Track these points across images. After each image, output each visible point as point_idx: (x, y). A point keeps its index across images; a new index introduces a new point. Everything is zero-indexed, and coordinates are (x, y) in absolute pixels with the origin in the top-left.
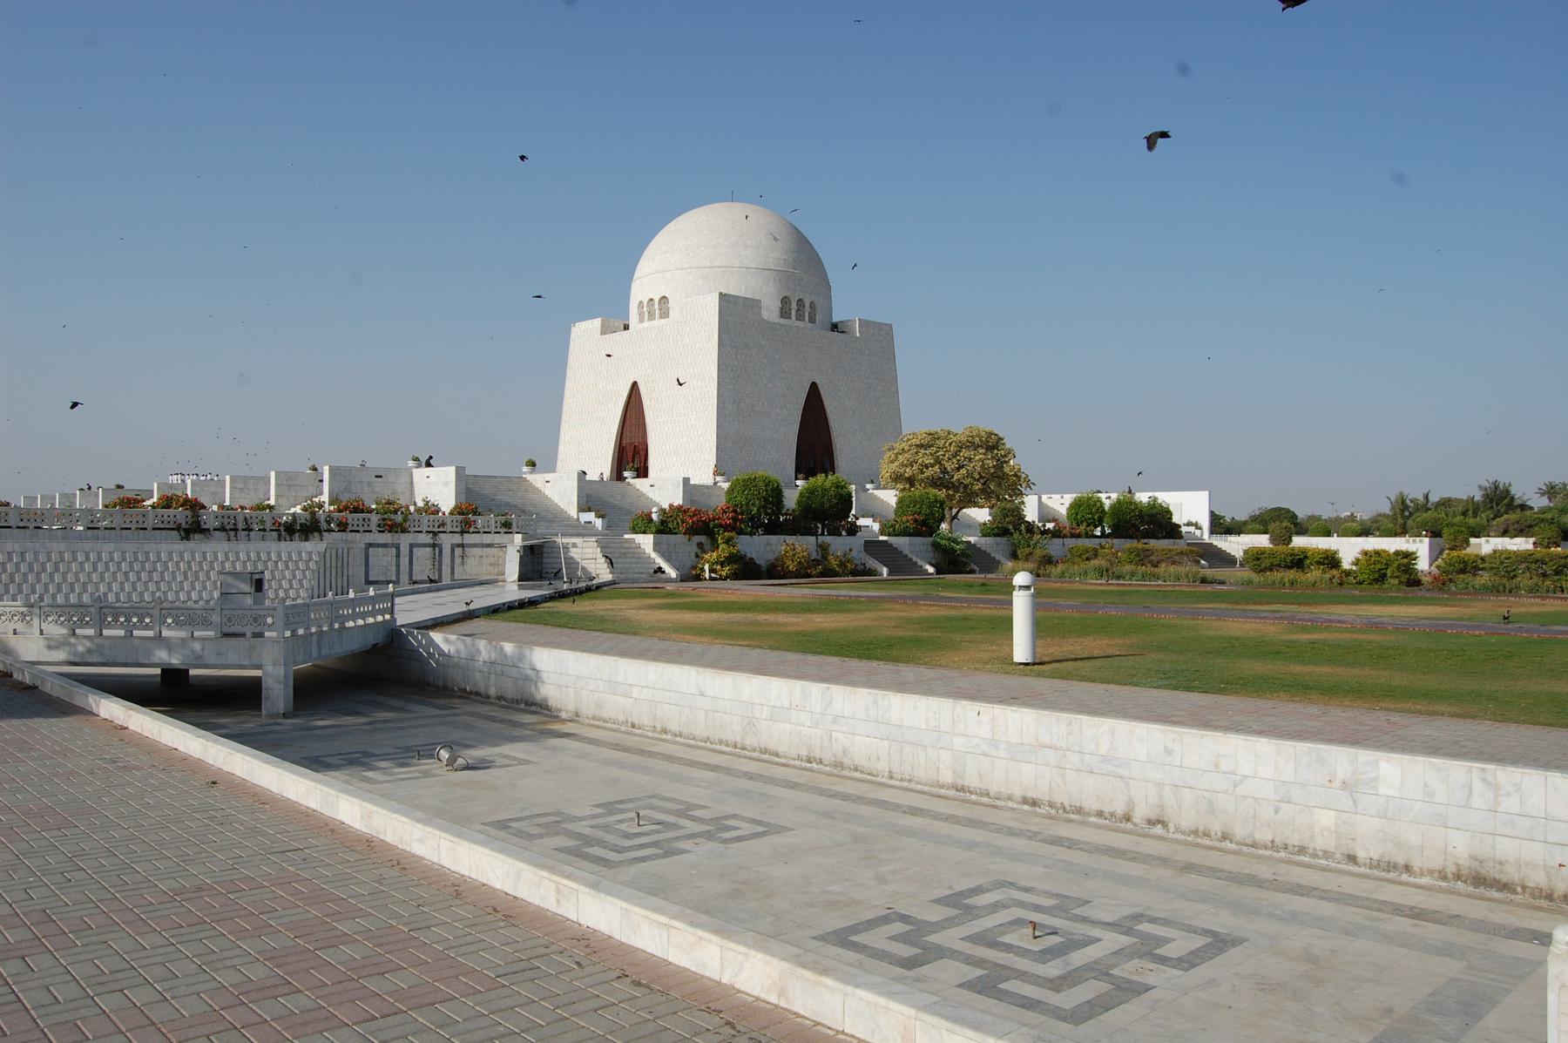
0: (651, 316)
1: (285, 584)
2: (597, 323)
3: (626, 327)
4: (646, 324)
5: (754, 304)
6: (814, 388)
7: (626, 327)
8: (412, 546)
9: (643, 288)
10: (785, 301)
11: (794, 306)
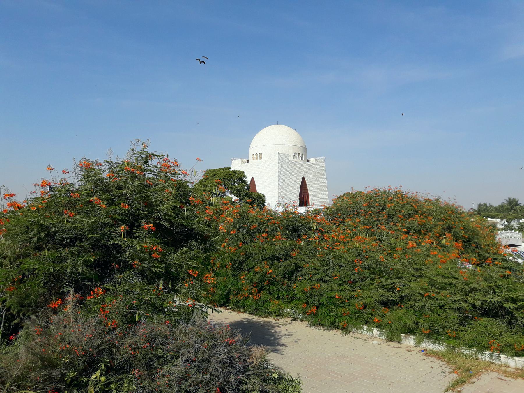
0: (257, 159)
2: (240, 160)
4: (255, 161)
5: (287, 156)
6: (303, 178)
7: (248, 161)
9: (253, 150)
11: (297, 155)
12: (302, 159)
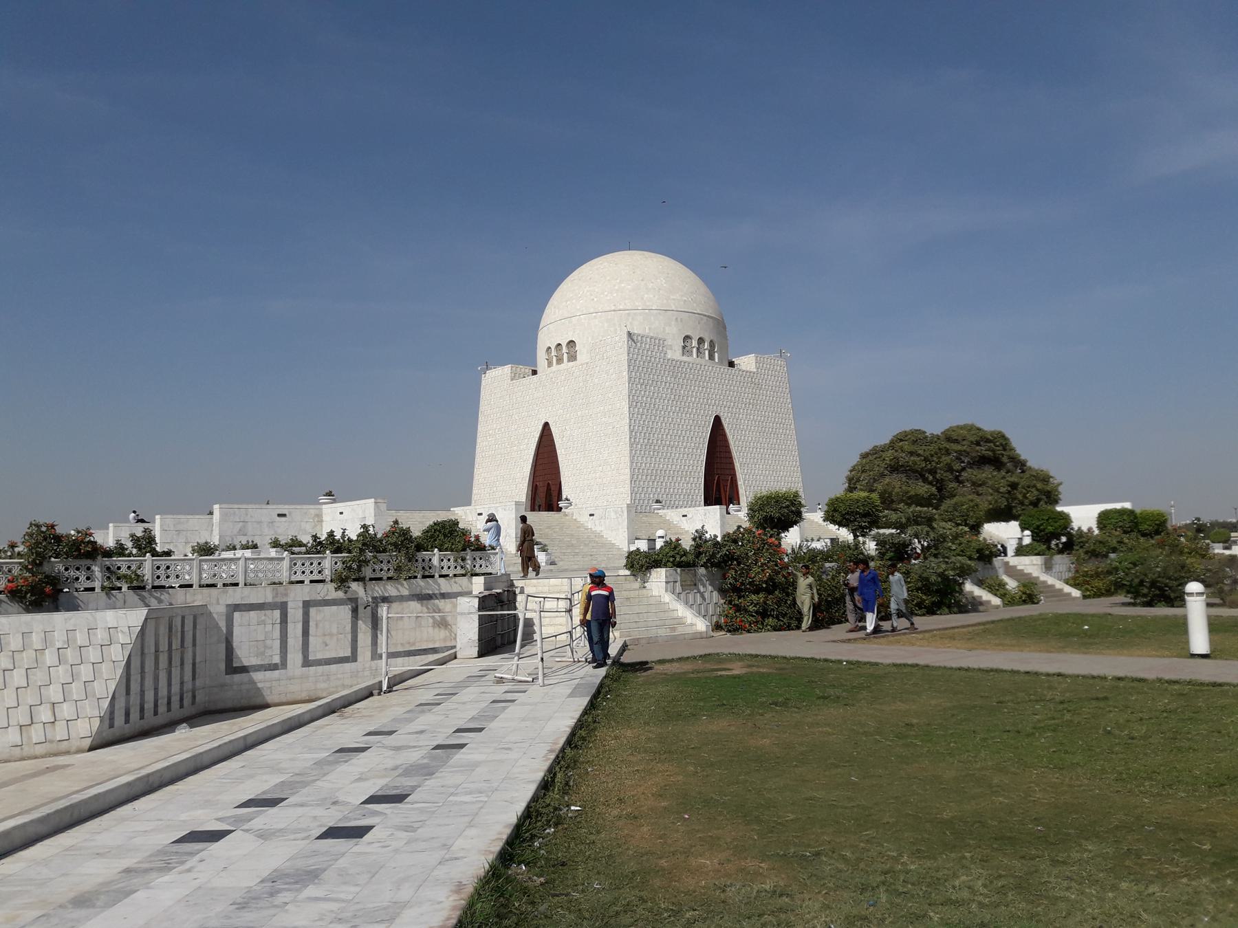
0: (560, 361)
1: (54, 693)
2: (507, 369)
3: (534, 373)
4: (555, 367)
5: (659, 343)
7: (534, 373)
8: (307, 605)
9: (551, 332)
10: (687, 338)
11: (695, 343)
12: (711, 357)
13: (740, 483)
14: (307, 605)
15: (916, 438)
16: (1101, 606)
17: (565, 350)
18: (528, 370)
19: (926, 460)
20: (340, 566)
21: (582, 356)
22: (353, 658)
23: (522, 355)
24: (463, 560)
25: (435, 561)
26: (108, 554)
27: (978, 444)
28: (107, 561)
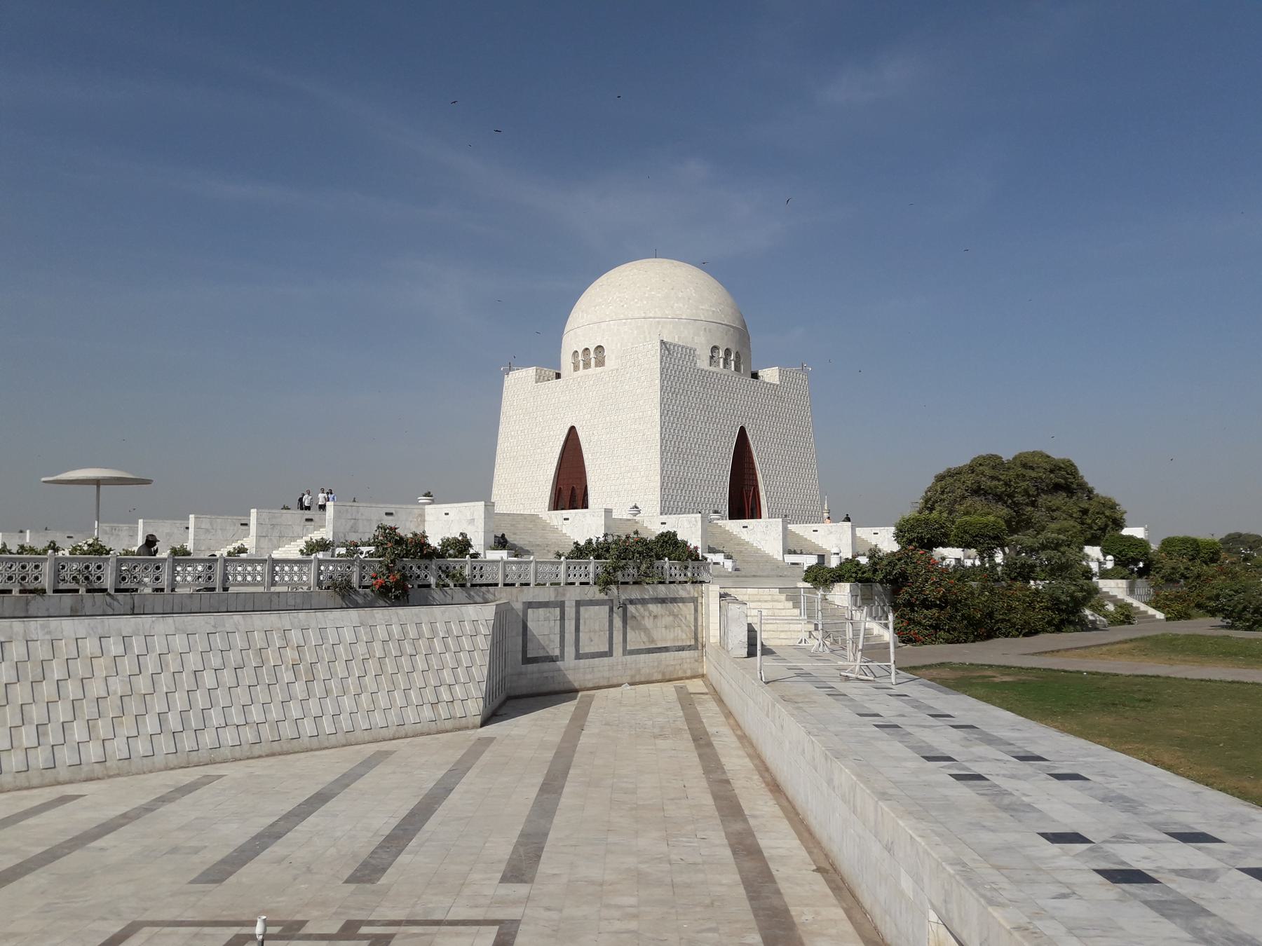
0: (587, 365)
1: (447, 676)
2: (532, 371)
4: (581, 372)
5: (690, 352)
7: (558, 376)
8: (579, 604)
10: (715, 348)
11: (722, 354)
12: (737, 369)
13: (762, 494)
14: (579, 604)
15: (994, 462)
16: (1182, 628)
17: (592, 355)
18: (552, 373)
19: (1007, 484)
20: (600, 570)
21: (611, 361)
22: (609, 653)
23: (546, 359)
24: (686, 568)
25: (666, 566)
26: (441, 555)
27: (1052, 471)
28: (440, 561)
